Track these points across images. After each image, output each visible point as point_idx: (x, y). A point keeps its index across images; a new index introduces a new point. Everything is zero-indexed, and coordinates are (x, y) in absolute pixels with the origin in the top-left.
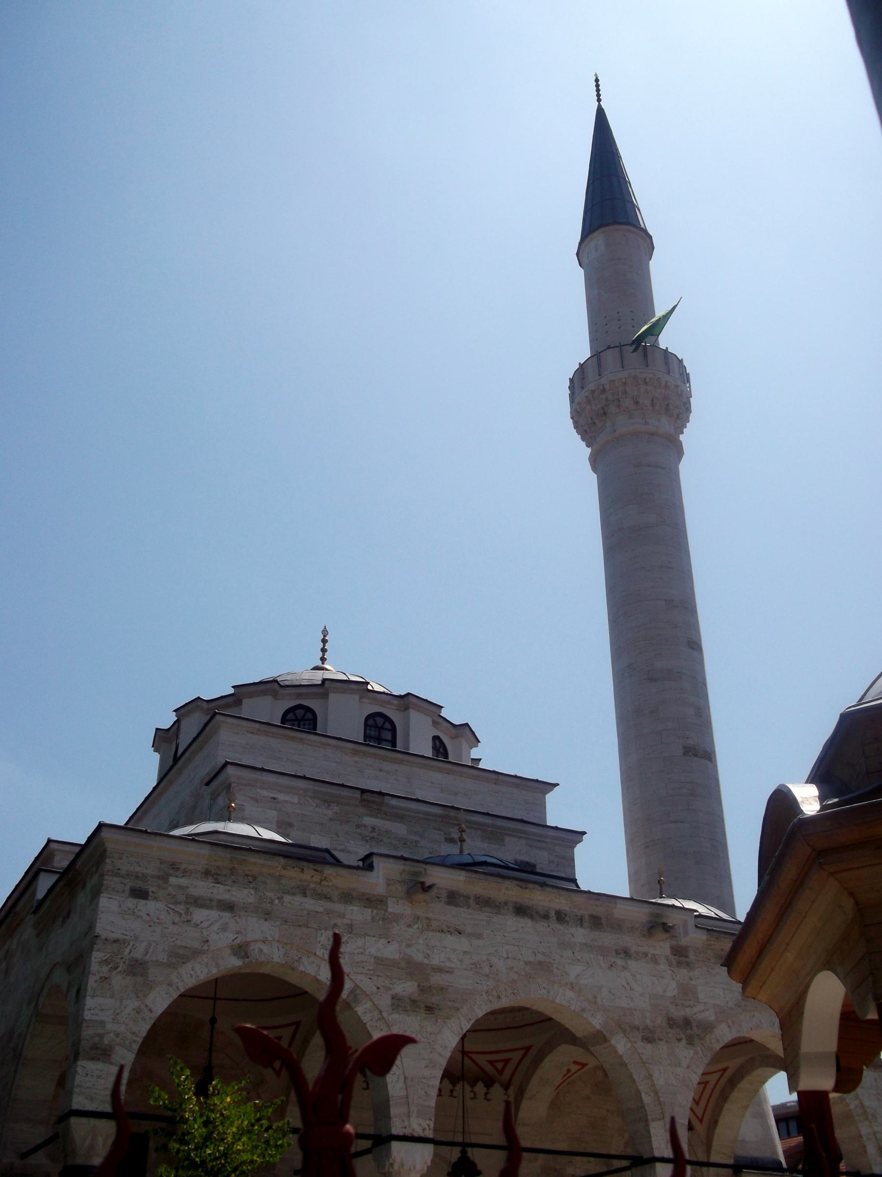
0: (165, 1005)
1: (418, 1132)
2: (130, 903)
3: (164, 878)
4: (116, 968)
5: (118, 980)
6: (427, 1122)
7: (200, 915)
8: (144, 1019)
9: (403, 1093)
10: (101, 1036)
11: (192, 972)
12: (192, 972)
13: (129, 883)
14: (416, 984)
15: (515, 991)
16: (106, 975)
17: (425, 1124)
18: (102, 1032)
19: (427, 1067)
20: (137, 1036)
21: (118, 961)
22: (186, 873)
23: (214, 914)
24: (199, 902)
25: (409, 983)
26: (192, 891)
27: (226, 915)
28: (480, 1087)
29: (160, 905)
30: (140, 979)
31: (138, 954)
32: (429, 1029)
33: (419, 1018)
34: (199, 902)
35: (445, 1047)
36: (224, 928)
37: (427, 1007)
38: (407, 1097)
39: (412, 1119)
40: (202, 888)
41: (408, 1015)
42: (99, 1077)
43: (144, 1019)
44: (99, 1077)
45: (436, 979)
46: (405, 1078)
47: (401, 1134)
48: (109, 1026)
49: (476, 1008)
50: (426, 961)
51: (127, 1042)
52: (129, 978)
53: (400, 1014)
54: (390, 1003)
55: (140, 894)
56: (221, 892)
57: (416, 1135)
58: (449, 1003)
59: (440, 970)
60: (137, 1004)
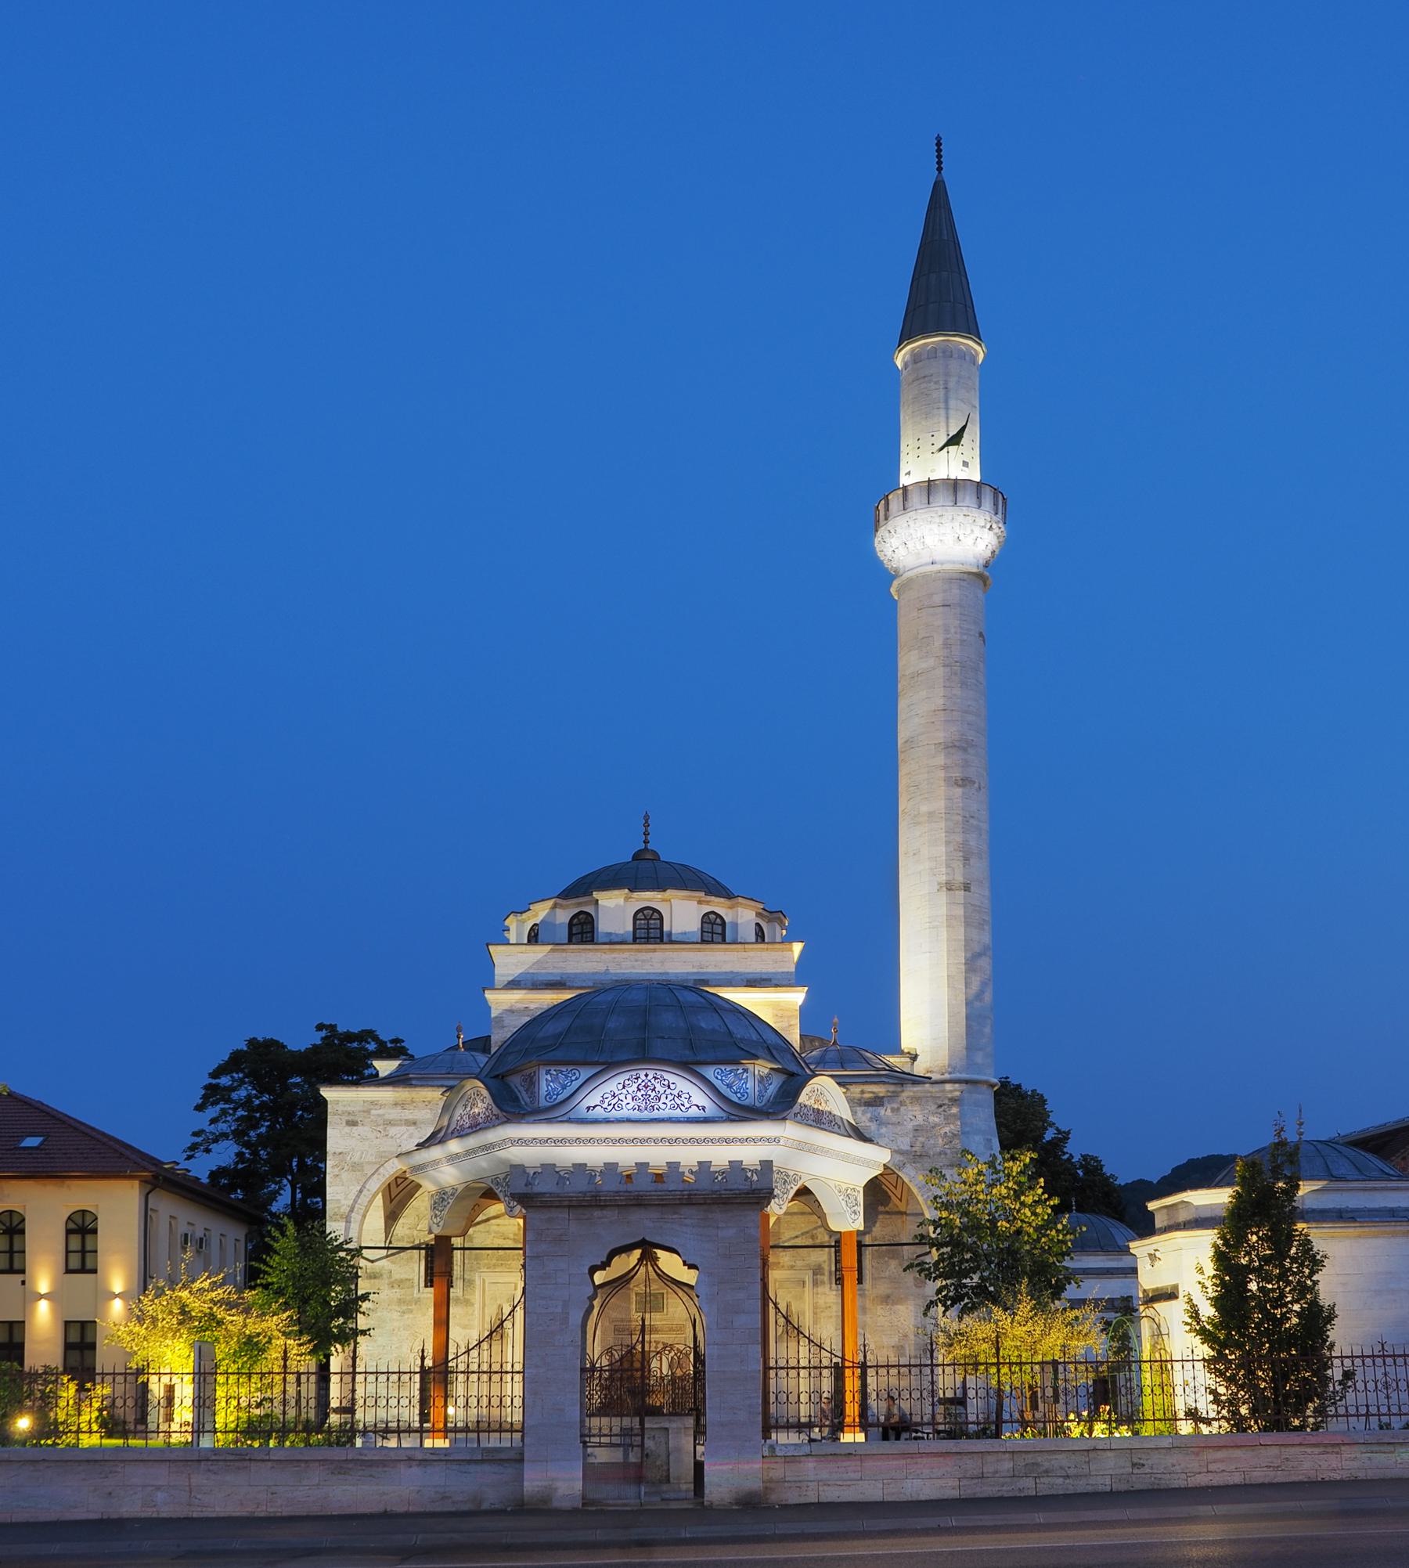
2: (347, 1129)
3: (368, 1112)
5: (345, 1175)
7: (393, 1131)
13: (345, 1118)
22: (381, 1106)
23: (404, 1128)
24: (390, 1123)
26: (387, 1117)
27: (412, 1128)
29: (366, 1128)
31: (356, 1159)
34: (390, 1123)
36: (411, 1136)
40: (394, 1114)
55: (352, 1123)
56: (408, 1115)
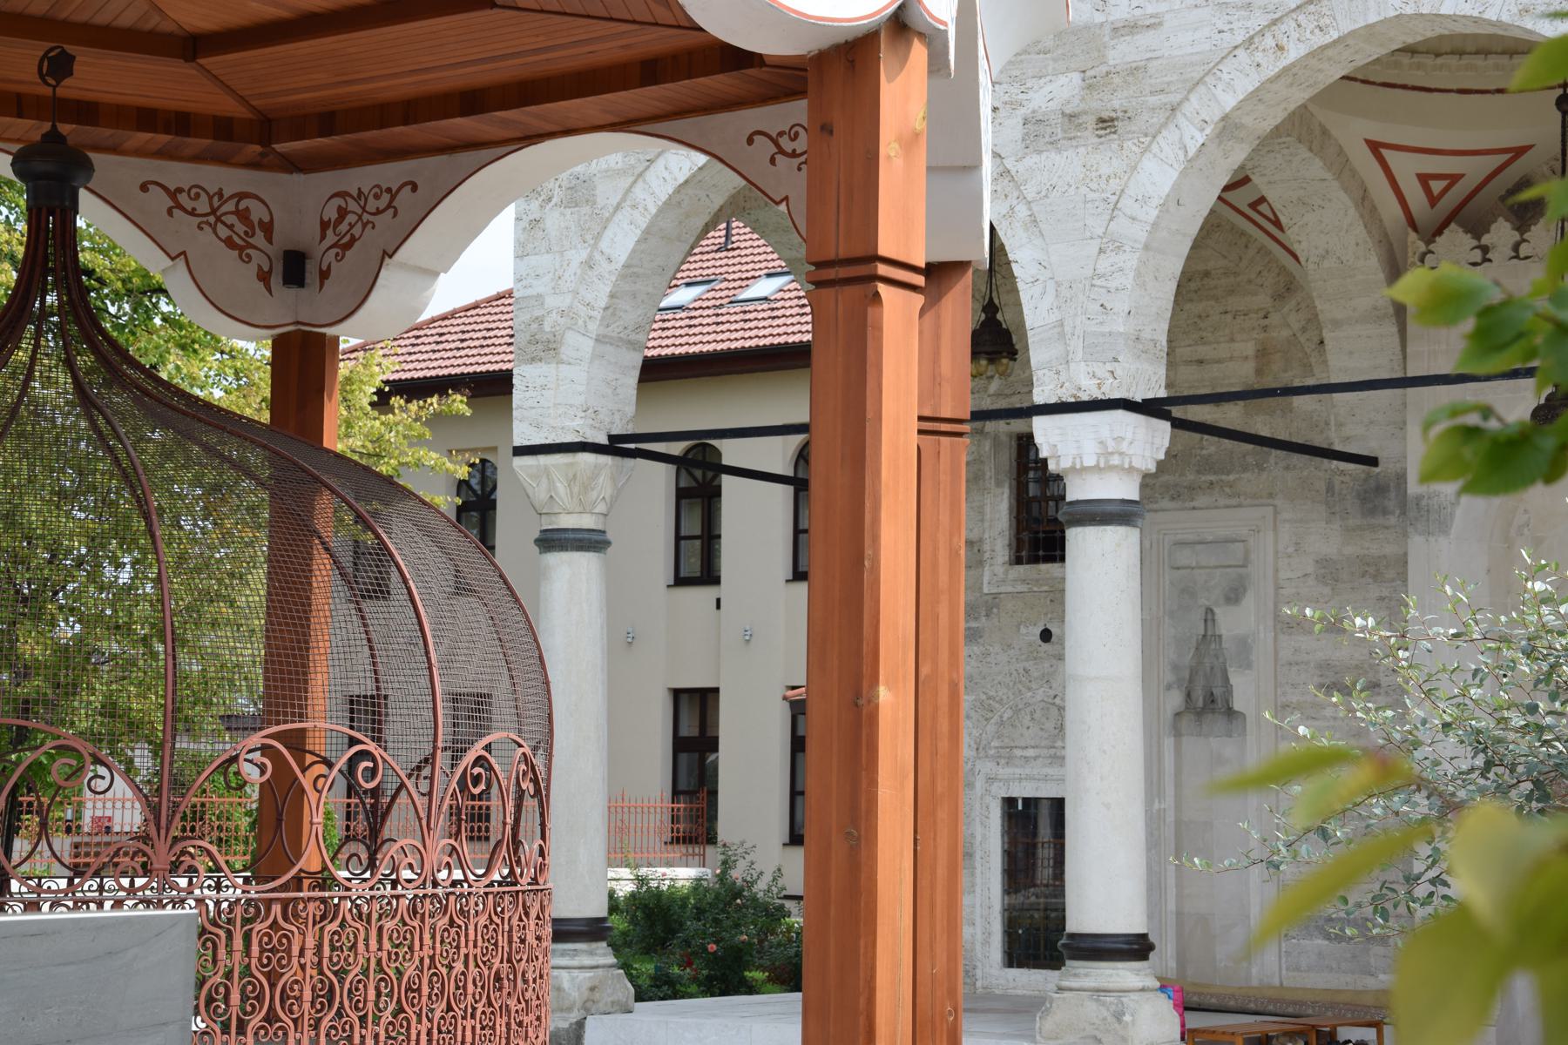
0: (630, 244)
1: (1090, 392)
4: (550, 200)
6: (1109, 367)
8: (600, 277)
9: (1054, 317)
10: (539, 320)
11: (666, 174)
12: (666, 174)
14: (1076, 77)
15: (1325, 21)
16: (537, 216)
17: (1102, 370)
18: (538, 313)
19: (1101, 251)
20: (593, 309)
21: (551, 186)
25: (1063, 80)
28: (1502, 233)
30: (586, 209)
32: (1105, 170)
33: (1082, 150)
35: (1143, 200)
37: (1102, 121)
38: (1061, 323)
39: (1072, 366)
41: (1059, 151)
42: (544, 387)
43: (600, 277)
44: (544, 387)
45: (1122, 53)
46: (1058, 284)
47: (1053, 401)
48: (551, 302)
49: (1218, 92)
50: (1099, 18)
51: (580, 322)
52: (568, 211)
53: (1040, 152)
54: (1020, 136)
57: (1085, 397)
58: (1153, 100)
59: (1132, 28)
60: (584, 255)
